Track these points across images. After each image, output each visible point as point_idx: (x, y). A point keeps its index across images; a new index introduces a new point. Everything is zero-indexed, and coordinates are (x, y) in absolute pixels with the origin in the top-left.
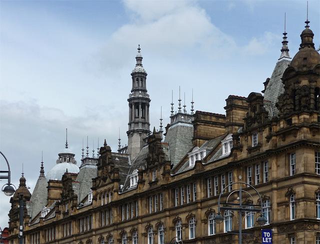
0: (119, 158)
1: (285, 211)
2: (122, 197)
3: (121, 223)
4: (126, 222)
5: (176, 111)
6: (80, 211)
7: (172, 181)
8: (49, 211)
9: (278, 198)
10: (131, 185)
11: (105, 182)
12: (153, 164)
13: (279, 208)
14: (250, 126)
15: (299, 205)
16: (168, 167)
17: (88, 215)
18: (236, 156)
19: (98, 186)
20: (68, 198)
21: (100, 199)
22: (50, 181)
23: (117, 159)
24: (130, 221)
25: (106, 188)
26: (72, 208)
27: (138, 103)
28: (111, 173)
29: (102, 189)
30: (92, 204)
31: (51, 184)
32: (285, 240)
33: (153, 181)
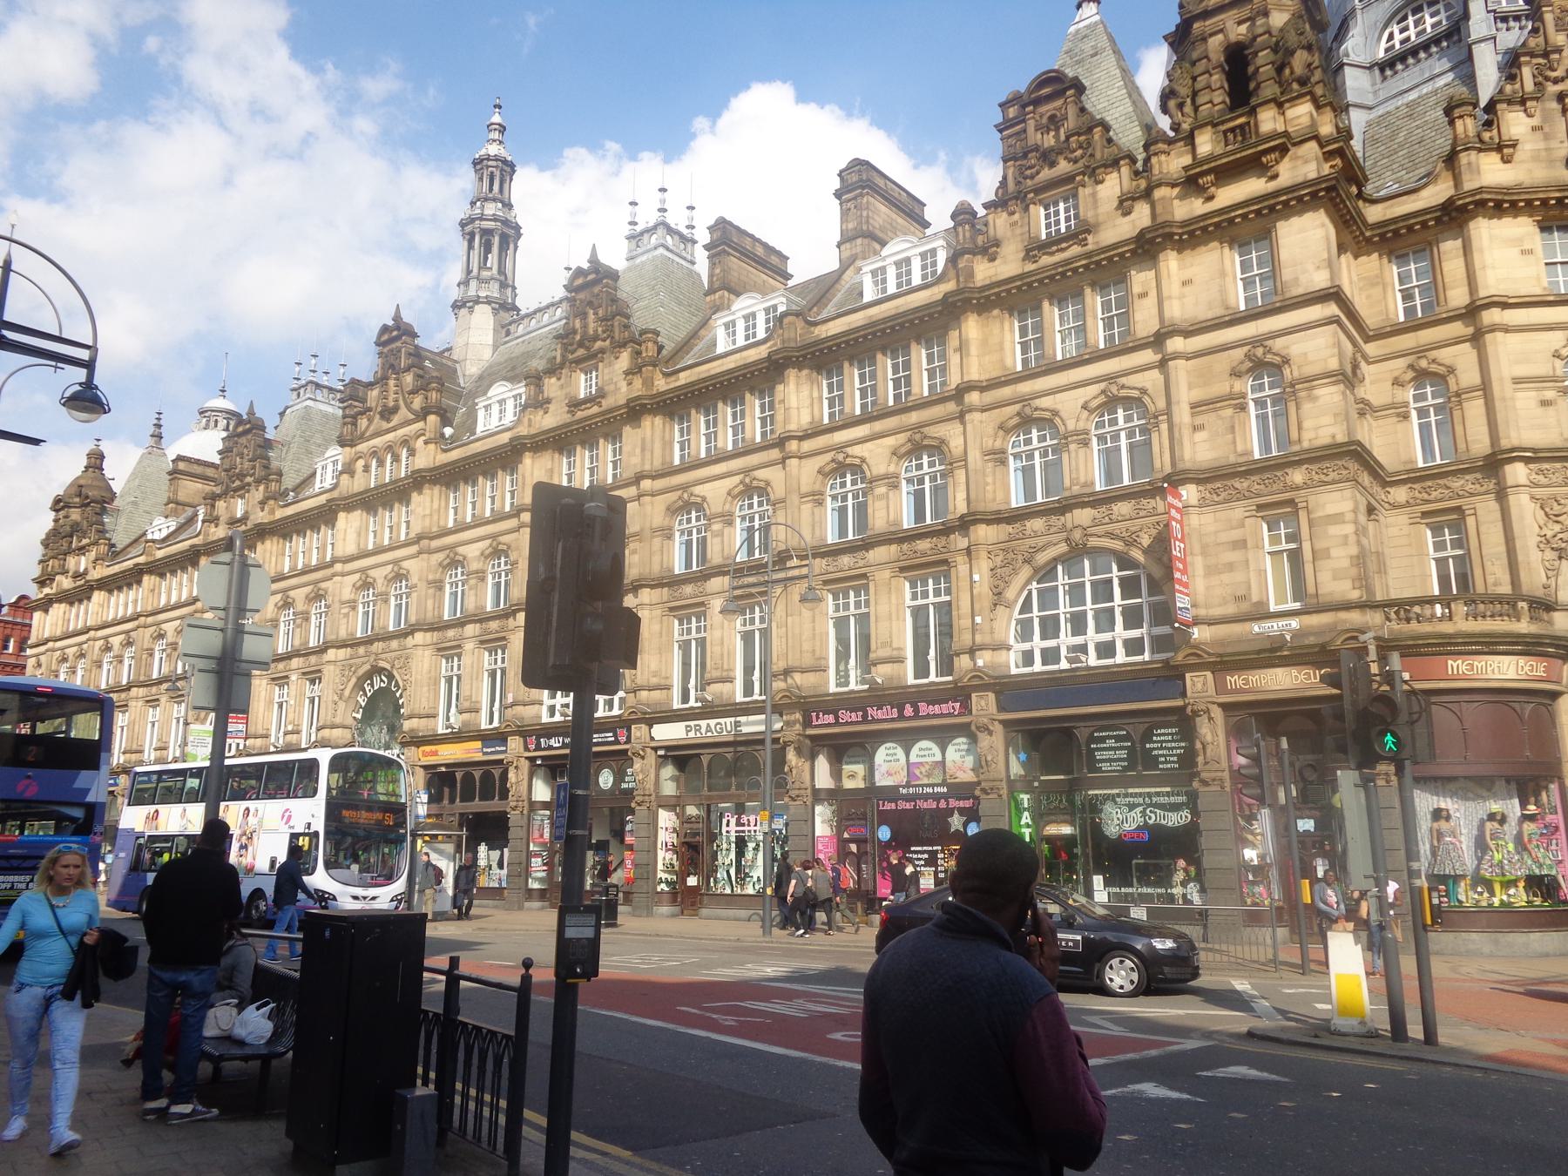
1: (1233, 427)
2: (455, 455)
3: (448, 532)
4: (461, 527)
5: (647, 217)
6: (290, 511)
7: (661, 384)
8: (172, 529)
9: (1190, 387)
10: (480, 428)
11: (388, 421)
12: (588, 349)
13: (1199, 420)
14: (1032, 177)
15: (1314, 399)
16: (649, 350)
17: (324, 516)
18: (971, 274)
19: (363, 434)
20: (249, 479)
21: (367, 469)
22: (180, 458)
24: (479, 522)
25: (390, 436)
26: (263, 503)
28: (412, 392)
29: (378, 442)
30: (335, 487)
31: (182, 466)
32: (1243, 526)
33: (582, 396)
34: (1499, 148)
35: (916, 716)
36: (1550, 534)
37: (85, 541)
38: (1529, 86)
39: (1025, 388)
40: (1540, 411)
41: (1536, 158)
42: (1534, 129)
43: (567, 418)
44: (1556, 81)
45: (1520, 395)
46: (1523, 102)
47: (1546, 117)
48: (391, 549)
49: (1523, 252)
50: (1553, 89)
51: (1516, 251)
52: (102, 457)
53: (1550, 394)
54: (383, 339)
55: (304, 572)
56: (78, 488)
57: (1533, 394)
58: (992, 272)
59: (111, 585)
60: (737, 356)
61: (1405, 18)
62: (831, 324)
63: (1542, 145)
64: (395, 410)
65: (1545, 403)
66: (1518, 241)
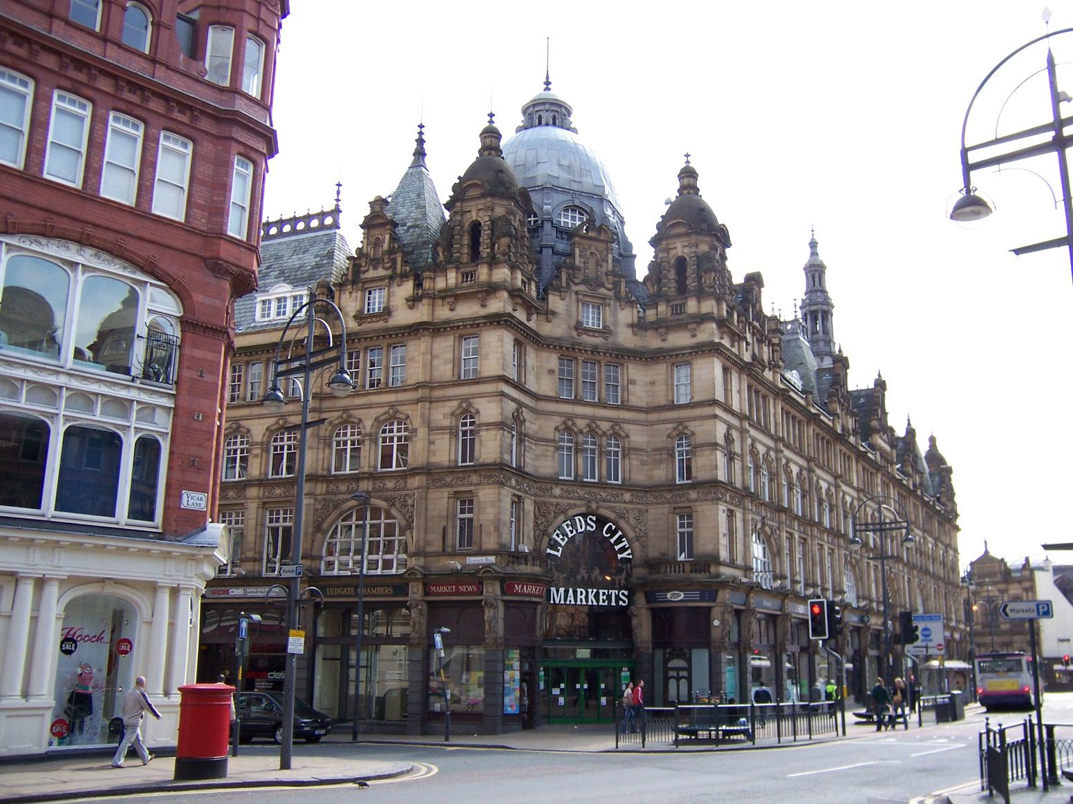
36: (539, 522)
38: (564, 284)
44: (576, 284)
50: (575, 288)
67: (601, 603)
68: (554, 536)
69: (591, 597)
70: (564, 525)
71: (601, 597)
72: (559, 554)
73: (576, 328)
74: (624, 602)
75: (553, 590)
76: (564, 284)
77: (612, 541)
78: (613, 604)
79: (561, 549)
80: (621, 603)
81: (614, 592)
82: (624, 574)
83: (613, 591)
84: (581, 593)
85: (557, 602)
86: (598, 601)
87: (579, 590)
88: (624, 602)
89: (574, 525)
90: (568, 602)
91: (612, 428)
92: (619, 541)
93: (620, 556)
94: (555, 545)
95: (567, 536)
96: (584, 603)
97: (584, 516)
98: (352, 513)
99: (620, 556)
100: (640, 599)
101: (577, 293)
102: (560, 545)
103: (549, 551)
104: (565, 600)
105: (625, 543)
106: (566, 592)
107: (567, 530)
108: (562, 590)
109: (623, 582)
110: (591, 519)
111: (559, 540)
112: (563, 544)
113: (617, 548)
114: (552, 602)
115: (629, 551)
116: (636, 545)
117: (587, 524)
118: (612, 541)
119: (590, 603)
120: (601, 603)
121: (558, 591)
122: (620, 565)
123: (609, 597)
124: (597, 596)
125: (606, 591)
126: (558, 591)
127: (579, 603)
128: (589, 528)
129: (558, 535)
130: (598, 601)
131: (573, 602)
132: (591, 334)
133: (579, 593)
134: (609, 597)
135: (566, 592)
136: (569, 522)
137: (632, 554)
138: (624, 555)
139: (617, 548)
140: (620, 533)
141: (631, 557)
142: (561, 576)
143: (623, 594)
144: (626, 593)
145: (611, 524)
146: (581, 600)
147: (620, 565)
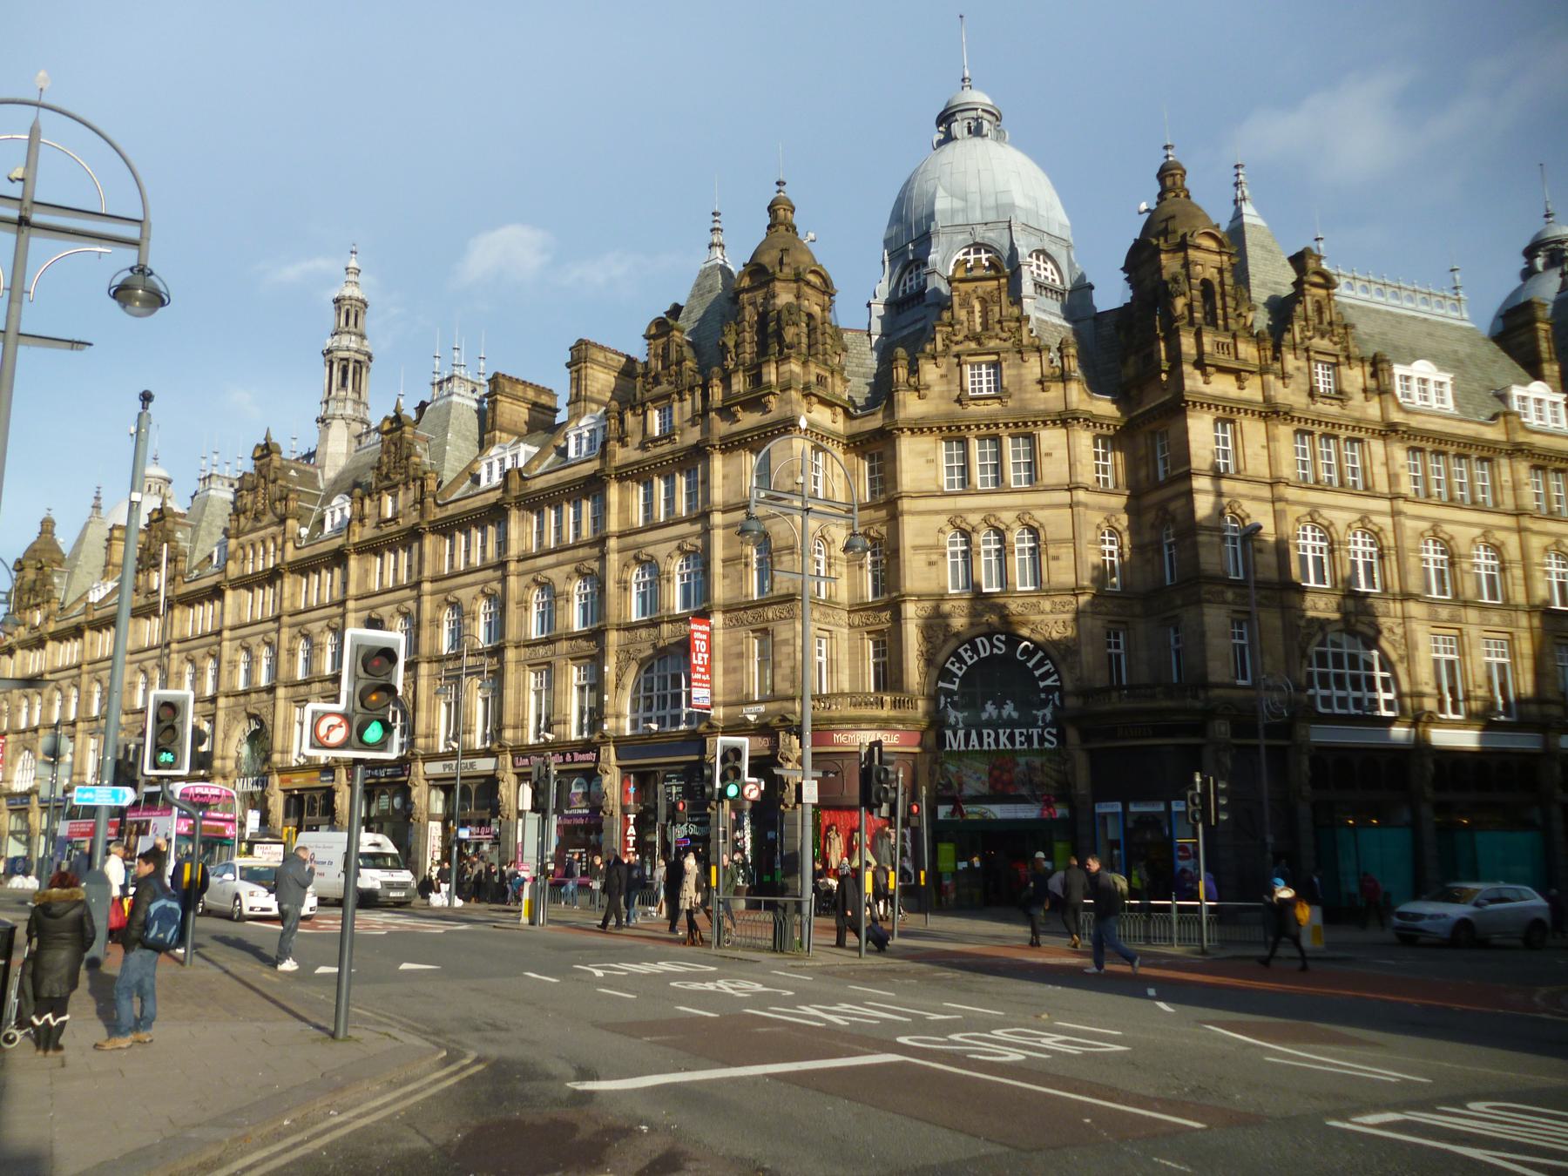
0: (297, 471)
2: (305, 553)
3: (301, 612)
23: (293, 473)
27: (347, 360)
29: (253, 536)
34: (917, 390)
35: (572, 762)
37: (39, 600)
38: (940, 347)
39: (640, 538)
40: (926, 569)
41: (941, 396)
42: (942, 376)
43: (377, 533)
44: (957, 343)
45: (916, 557)
46: (934, 358)
47: (949, 369)
48: (261, 622)
49: (928, 461)
50: (955, 349)
51: (924, 460)
52: (53, 523)
53: (934, 557)
54: (257, 455)
55: (202, 636)
56: (32, 551)
57: (924, 557)
58: (626, 454)
59: (60, 637)
60: (482, 496)
61: (911, 273)
62: (537, 480)
63: (945, 388)
64: (264, 513)
65: (931, 564)
66: (924, 453)
67: (1018, 746)
68: (948, 665)
69: (1003, 739)
70: (961, 650)
71: (1018, 739)
72: (955, 687)
73: (959, 401)
74: (1052, 743)
75: (949, 733)
76: (940, 347)
77: (1030, 665)
78: (1036, 745)
79: (957, 680)
80: (1047, 745)
81: (1035, 732)
82: (1050, 706)
83: (1035, 731)
84: (989, 735)
85: (955, 747)
86: (1012, 742)
87: (985, 732)
88: (1052, 743)
89: (975, 650)
90: (970, 748)
91: (1019, 518)
92: (1039, 664)
93: (1042, 684)
94: (945, 675)
95: (966, 663)
96: (993, 747)
97: (989, 636)
98: (652, 665)
99: (1042, 684)
100: (1072, 735)
101: (958, 356)
102: (956, 675)
103: (941, 684)
104: (967, 744)
105: (1049, 666)
106: (967, 737)
107: (966, 656)
108: (961, 733)
109: (1049, 717)
110: (998, 639)
111: (954, 669)
112: (960, 674)
113: (1037, 673)
114: (948, 748)
115: (1055, 677)
116: (1063, 669)
117: (993, 646)
118: (1030, 665)
119: (1002, 747)
120: (1018, 746)
121: (955, 735)
122: (1043, 696)
123: (1029, 739)
124: (1011, 738)
125: (1024, 731)
126: (955, 735)
127: (986, 747)
128: (995, 651)
129: (953, 664)
130: (1012, 742)
131: (977, 747)
132: (982, 402)
133: (985, 736)
134: (1029, 739)
135: (967, 737)
136: (967, 646)
137: (1060, 679)
138: (1049, 682)
139: (1037, 673)
140: (1040, 654)
141: (1058, 684)
142: (960, 716)
143: (1049, 733)
144: (1054, 731)
145: (1026, 643)
146: (989, 744)
147: (1043, 696)
